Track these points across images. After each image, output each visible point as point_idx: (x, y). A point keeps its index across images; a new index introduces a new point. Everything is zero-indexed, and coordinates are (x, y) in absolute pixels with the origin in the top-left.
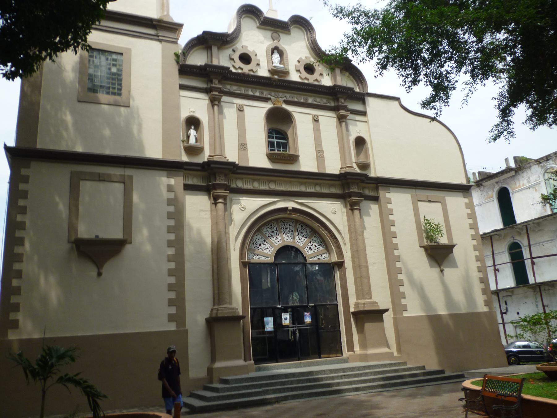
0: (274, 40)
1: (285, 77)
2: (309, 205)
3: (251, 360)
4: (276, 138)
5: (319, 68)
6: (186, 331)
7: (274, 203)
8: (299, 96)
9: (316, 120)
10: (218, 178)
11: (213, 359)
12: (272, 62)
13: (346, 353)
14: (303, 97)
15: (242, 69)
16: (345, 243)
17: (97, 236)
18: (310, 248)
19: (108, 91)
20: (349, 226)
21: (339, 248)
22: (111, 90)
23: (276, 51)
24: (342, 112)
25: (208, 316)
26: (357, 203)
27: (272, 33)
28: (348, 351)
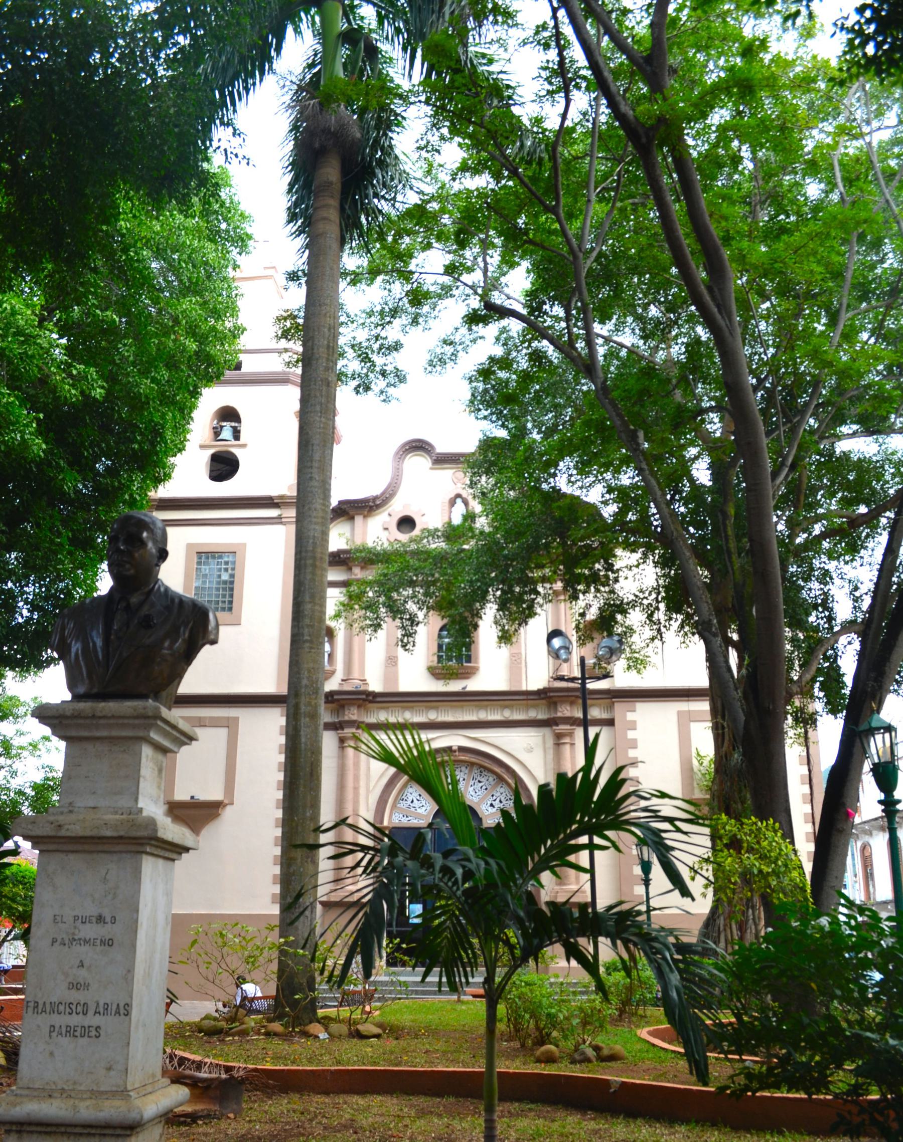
18: (492, 805)
23: (459, 501)
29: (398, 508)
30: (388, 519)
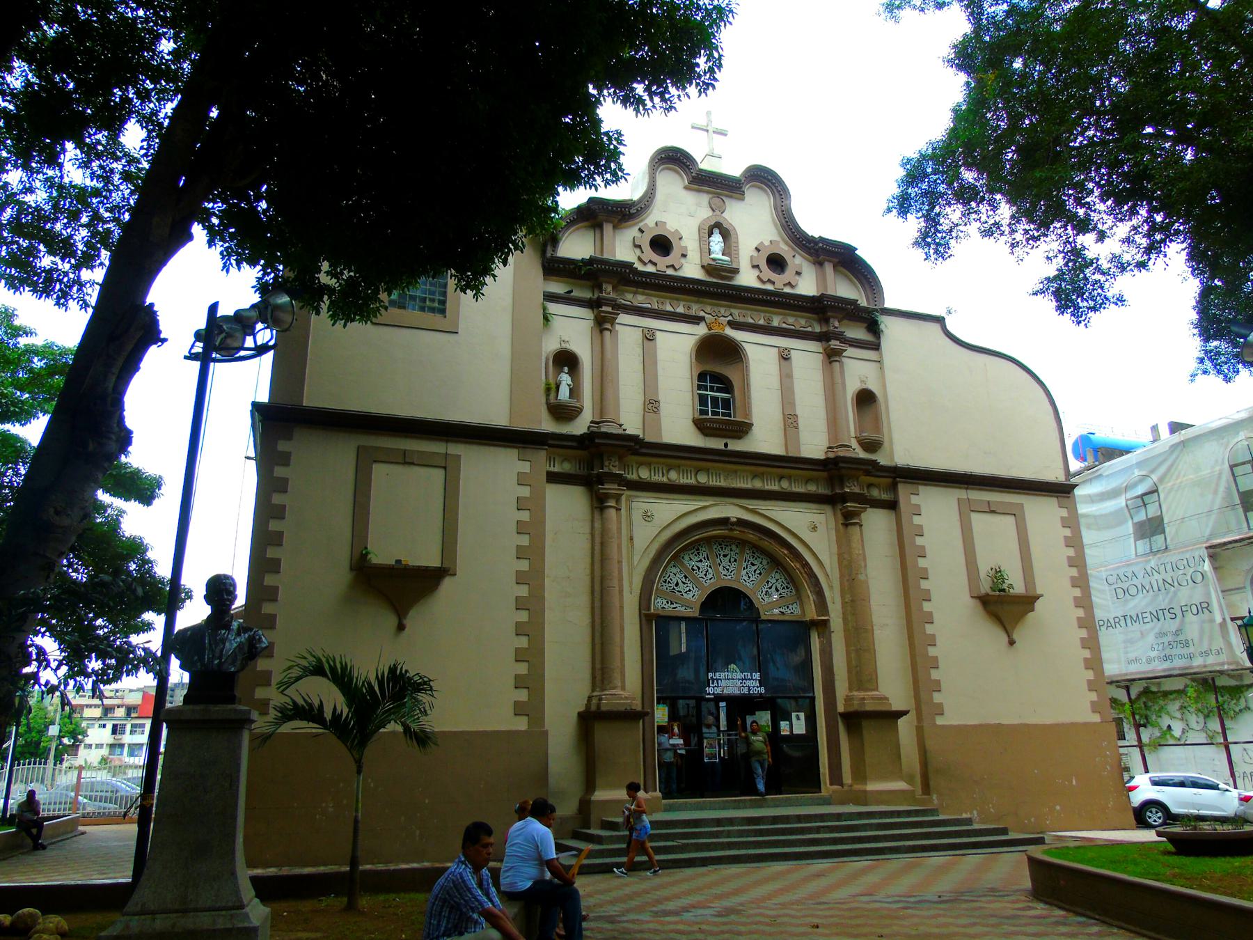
0: (713, 211)
1: (731, 278)
2: (767, 513)
3: (655, 790)
4: (712, 389)
5: (796, 260)
6: (545, 733)
7: (705, 507)
8: (755, 313)
9: (785, 357)
10: (606, 463)
11: (590, 784)
12: (709, 249)
13: (827, 788)
14: (762, 315)
15: (655, 264)
16: (832, 586)
17: (398, 562)
19: (422, 304)
20: (840, 555)
21: (819, 593)
22: (428, 303)
23: (716, 231)
24: (834, 344)
25: (582, 709)
26: (856, 514)
27: (712, 198)
28: (831, 784)
29: (651, 220)
30: (638, 234)
